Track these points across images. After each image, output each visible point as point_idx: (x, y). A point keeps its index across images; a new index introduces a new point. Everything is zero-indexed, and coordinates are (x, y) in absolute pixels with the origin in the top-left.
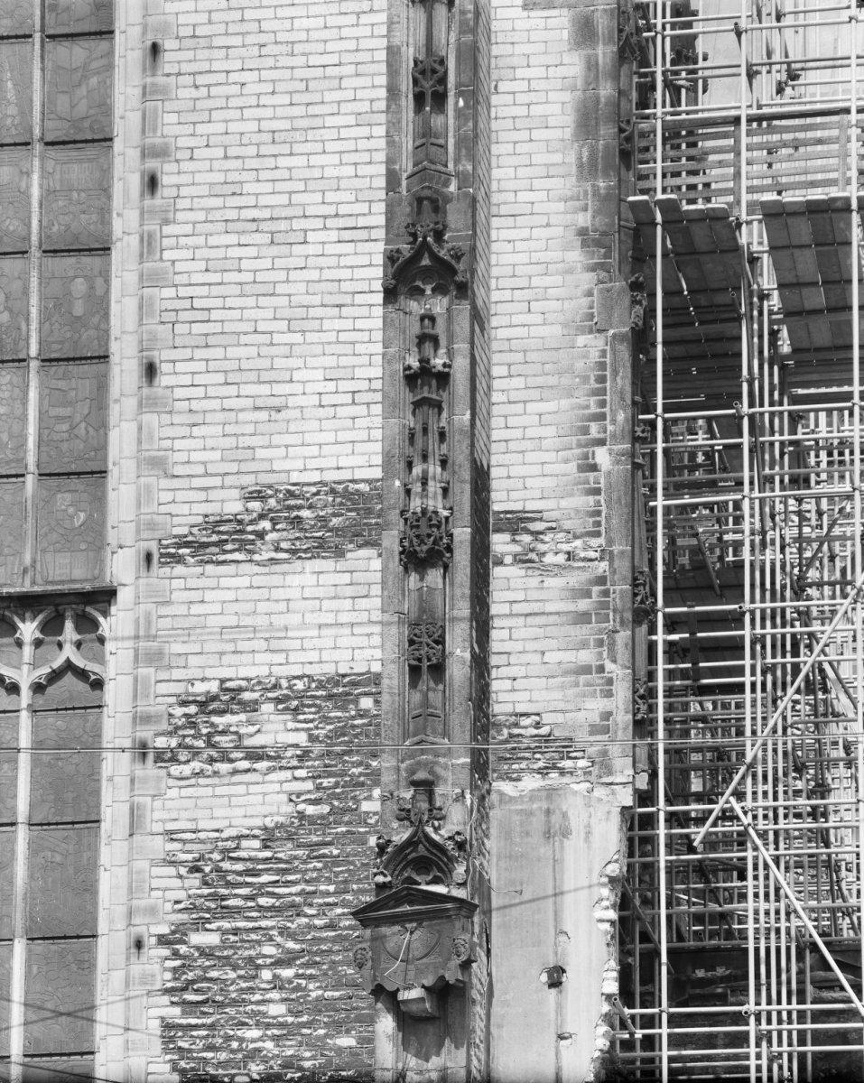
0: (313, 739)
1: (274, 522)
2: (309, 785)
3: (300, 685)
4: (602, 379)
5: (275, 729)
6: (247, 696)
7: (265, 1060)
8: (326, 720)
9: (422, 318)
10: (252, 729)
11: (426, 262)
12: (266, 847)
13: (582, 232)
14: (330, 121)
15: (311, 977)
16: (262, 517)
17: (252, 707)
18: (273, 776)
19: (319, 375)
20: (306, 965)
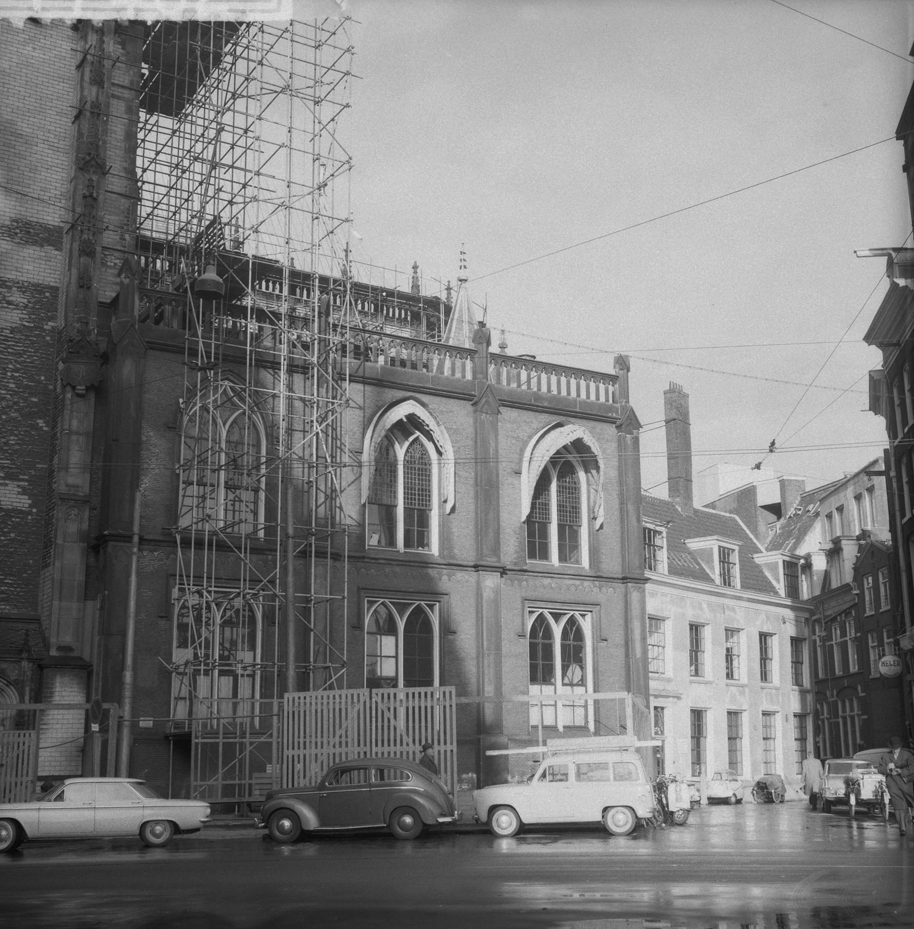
0: (29, 302)
1: (21, 231)
2: (27, 317)
3: (26, 284)
4: (128, 214)
5: (17, 297)
6: (8, 284)
7: (7, 401)
8: (35, 297)
9: (89, 180)
10: (9, 295)
11: (93, 163)
12: (11, 333)
13: (125, 168)
14: (48, 111)
15: (24, 377)
16: (17, 228)
17: (10, 288)
18: (15, 311)
19: (39, 188)
20: (22, 373)
